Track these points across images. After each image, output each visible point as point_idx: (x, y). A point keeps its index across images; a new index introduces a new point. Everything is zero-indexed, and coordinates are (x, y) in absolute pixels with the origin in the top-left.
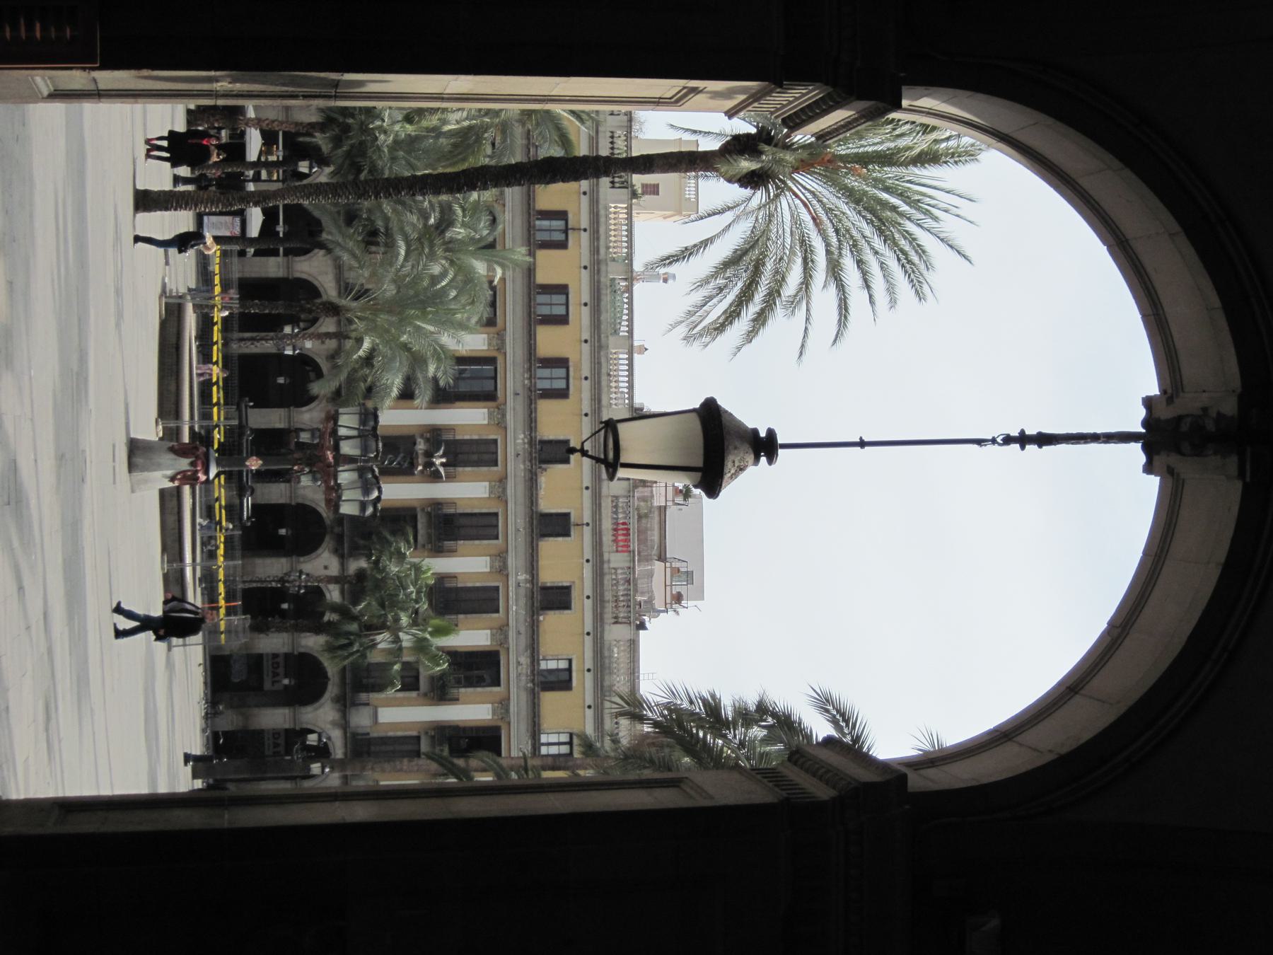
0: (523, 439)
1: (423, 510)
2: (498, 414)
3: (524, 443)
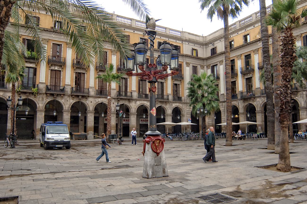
0: (53, 35)
1: (75, 70)
2: (44, 41)
3: (55, 35)
